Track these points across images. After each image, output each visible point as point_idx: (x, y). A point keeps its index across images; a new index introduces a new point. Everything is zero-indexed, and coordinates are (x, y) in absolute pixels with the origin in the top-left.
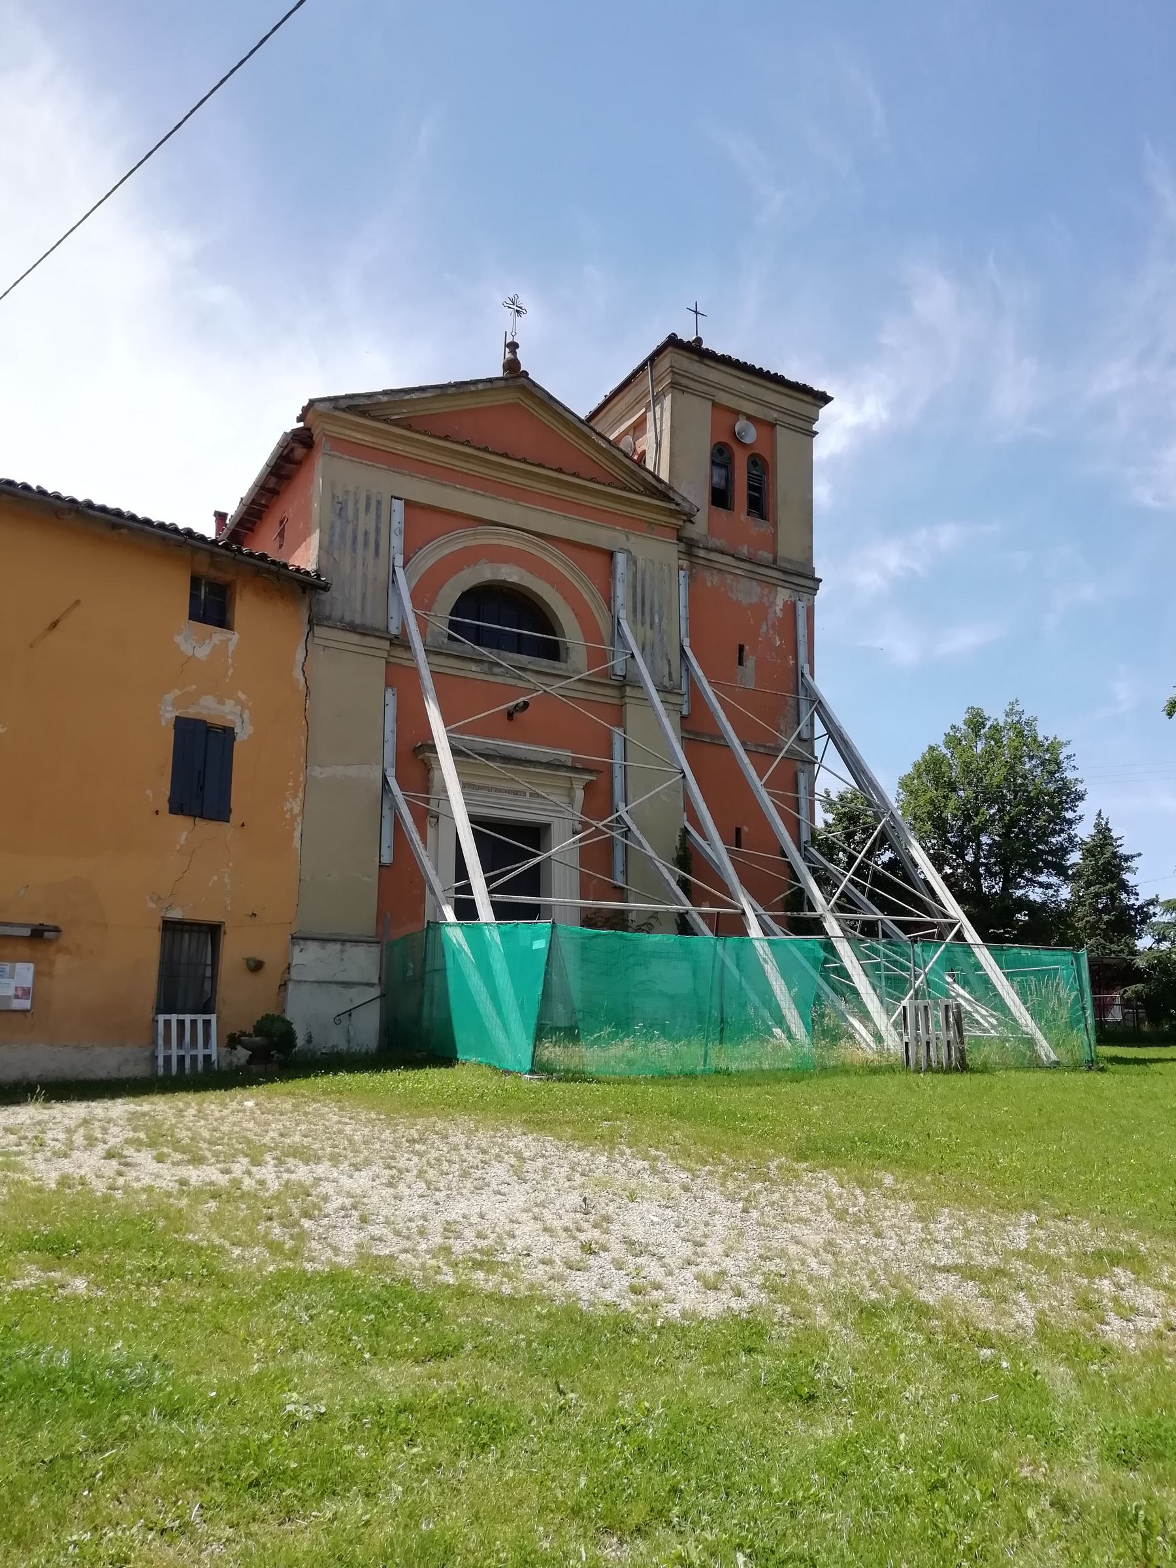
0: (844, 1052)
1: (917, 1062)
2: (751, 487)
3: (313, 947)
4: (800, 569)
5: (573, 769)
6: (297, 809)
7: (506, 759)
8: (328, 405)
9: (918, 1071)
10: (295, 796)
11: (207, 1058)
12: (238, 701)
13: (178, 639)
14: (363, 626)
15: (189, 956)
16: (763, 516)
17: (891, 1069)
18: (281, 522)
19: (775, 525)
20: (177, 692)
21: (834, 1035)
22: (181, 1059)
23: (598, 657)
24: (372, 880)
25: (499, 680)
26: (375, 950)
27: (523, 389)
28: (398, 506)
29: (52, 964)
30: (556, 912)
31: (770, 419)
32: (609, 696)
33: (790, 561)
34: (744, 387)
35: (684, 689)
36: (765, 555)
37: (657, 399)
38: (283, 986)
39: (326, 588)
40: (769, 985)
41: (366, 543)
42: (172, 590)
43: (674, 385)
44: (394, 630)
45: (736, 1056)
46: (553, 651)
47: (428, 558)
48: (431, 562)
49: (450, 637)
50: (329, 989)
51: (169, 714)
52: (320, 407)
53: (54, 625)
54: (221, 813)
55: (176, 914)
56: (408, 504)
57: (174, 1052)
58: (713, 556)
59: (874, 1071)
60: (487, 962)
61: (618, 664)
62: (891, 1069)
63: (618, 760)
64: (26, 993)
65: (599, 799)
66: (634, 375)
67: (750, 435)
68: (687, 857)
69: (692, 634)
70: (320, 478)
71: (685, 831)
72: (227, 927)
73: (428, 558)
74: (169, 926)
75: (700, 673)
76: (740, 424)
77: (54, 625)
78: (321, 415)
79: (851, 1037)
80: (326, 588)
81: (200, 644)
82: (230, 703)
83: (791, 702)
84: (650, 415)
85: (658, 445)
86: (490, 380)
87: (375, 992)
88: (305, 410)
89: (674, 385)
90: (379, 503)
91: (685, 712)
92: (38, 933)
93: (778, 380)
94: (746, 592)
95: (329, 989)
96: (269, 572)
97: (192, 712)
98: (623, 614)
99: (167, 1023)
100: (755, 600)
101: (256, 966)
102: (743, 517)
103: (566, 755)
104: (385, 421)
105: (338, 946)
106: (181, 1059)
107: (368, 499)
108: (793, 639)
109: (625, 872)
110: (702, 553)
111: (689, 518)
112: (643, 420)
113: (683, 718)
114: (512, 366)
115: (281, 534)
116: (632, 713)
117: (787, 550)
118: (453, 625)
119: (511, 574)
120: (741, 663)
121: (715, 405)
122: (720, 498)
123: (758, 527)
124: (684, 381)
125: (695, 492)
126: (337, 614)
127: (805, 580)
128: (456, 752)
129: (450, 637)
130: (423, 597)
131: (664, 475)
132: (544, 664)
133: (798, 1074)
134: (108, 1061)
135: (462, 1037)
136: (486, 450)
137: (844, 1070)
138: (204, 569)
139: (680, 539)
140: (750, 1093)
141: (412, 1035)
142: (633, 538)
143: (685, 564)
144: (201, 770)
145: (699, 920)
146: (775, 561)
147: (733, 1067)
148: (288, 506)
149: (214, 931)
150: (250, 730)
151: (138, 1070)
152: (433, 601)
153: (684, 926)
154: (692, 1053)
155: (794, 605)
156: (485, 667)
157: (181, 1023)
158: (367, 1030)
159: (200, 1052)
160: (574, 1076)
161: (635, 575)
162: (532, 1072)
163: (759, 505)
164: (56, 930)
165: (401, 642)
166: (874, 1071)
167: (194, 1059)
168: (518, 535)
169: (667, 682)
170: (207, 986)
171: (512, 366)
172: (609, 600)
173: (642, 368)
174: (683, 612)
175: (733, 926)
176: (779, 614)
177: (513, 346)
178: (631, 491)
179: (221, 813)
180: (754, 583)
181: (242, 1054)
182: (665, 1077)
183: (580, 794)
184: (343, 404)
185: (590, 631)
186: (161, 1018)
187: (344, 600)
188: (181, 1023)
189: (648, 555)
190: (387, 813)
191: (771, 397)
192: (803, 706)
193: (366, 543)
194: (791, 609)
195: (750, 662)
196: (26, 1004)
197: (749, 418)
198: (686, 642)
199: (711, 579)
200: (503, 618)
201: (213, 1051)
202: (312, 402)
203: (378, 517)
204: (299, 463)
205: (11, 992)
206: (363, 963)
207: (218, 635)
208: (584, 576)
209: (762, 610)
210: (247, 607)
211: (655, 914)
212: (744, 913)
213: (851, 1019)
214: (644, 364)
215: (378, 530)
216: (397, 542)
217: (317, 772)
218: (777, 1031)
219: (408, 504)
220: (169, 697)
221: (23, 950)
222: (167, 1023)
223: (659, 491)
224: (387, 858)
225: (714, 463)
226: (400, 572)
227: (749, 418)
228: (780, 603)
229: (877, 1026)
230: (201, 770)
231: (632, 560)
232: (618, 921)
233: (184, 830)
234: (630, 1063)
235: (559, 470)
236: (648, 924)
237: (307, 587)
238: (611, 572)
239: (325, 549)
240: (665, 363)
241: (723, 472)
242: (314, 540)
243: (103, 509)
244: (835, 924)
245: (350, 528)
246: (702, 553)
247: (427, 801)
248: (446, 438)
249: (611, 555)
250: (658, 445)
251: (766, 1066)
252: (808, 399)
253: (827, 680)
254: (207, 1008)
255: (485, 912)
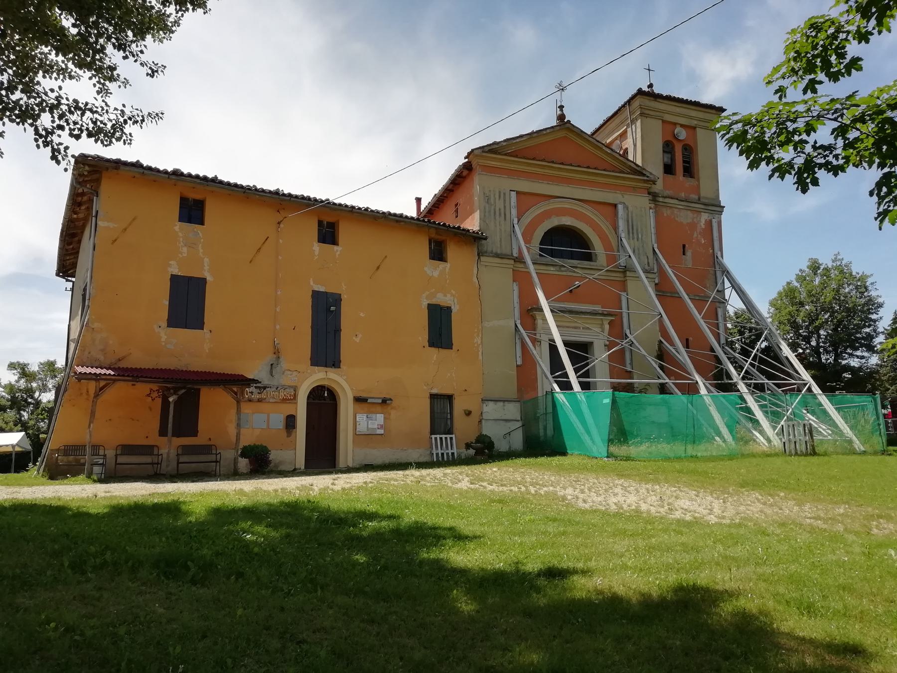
0: (752, 448)
1: (790, 451)
2: (684, 162)
3: (491, 404)
4: (713, 202)
5: (603, 314)
6: (479, 342)
7: (571, 312)
8: (480, 151)
9: (791, 455)
10: (478, 336)
11: (453, 454)
12: (452, 295)
13: (426, 269)
14: (501, 254)
15: (441, 408)
16: (692, 176)
17: (776, 455)
18: (456, 205)
19: (698, 181)
20: (427, 293)
21: (747, 440)
22: (442, 454)
23: (612, 259)
24: (514, 373)
25: (564, 273)
26: (518, 405)
27: (568, 128)
28: (513, 194)
29: (390, 414)
30: (598, 385)
31: (693, 125)
32: (618, 277)
33: (706, 198)
34: (678, 110)
35: (656, 270)
36: (694, 197)
37: (633, 122)
38: (480, 422)
39: (486, 239)
40: (712, 417)
41: (500, 214)
42: (422, 247)
43: (642, 114)
44: (515, 255)
45: (701, 450)
46: (589, 257)
47: (528, 218)
48: (529, 219)
49: (541, 255)
50: (501, 421)
51: (425, 303)
52: (476, 152)
53: (378, 268)
54: (449, 346)
55: (435, 391)
56: (518, 193)
57: (440, 452)
58: (667, 200)
59: (768, 455)
60: (583, 410)
61: (622, 261)
62: (776, 455)
63: (624, 310)
64: (382, 426)
65: (617, 330)
66: (620, 109)
67: (682, 134)
68: (662, 355)
69: (658, 242)
70: (478, 185)
71: (661, 342)
72: (455, 396)
73: (528, 218)
74: (433, 397)
75: (664, 262)
76: (678, 130)
77: (378, 268)
78: (477, 156)
79: (755, 441)
80: (486, 239)
81: (435, 269)
82: (449, 295)
83: (712, 272)
84: (629, 130)
85: (635, 145)
86: (552, 127)
87: (519, 424)
88: (469, 154)
89: (642, 114)
90: (504, 194)
91: (657, 281)
92: (384, 401)
93: (697, 104)
94: (684, 217)
95: (501, 421)
96: (462, 234)
97: (434, 301)
98: (623, 235)
99: (436, 439)
100: (689, 221)
101: (468, 413)
102: (681, 178)
103: (598, 308)
104: (505, 155)
105: (501, 404)
106: (442, 454)
107: (500, 192)
108: (711, 237)
109: (631, 364)
110: (661, 199)
111: (654, 182)
112: (625, 132)
113: (656, 284)
114: (561, 117)
115: (457, 211)
116: (630, 284)
117: (705, 192)
118: (541, 249)
119: (567, 221)
120: (684, 254)
121: (664, 122)
122: (669, 169)
123: (689, 182)
124: (647, 112)
125: (656, 169)
126: (490, 249)
127: (716, 207)
128: (552, 311)
129: (541, 255)
130: (527, 238)
131: (639, 162)
132: (586, 264)
133: (731, 457)
134: (415, 455)
135: (569, 443)
136: (553, 162)
137: (753, 456)
138: (433, 236)
139: (649, 193)
140: (711, 465)
141: (542, 441)
142: (626, 196)
143: (652, 206)
144: (440, 327)
145: (673, 386)
146: (699, 199)
147: (699, 455)
148: (460, 197)
149: (450, 398)
150: (457, 307)
151: (422, 460)
152: (531, 239)
153: (663, 389)
154: (678, 448)
155: (711, 221)
156: (558, 268)
157: (441, 439)
158: (517, 441)
159: (450, 452)
160: (628, 459)
161: (628, 215)
162: (608, 457)
163: (689, 170)
164: (391, 400)
165: (520, 260)
166: (768, 455)
167: (448, 454)
168: (570, 201)
169: (647, 267)
170: (449, 422)
171: (561, 117)
172: (616, 228)
173: (624, 106)
174: (653, 231)
175: (691, 389)
176: (703, 226)
177: (561, 107)
178: (624, 173)
179: (449, 346)
180: (689, 212)
181: (472, 452)
182: (667, 459)
183: (607, 327)
184: (487, 149)
185: (607, 246)
186: (433, 436)
187: (493, 243)
188: (441, 439)
189: (635, 204)
190: (518, 342)
191: (694, 113)
192: (719, 274)
193: (500, 214)
194: (709, 224)
195: (689, 253)
196: (382, 432)
197: (682, 126)
198: (656, 246)
199: (666, 212)
200: (564, 243)
201: (455, 450)
202: (473, 150)
203: (505, 201)
204: (465, 177)
205: (376, 427)
206: (513, 411)
207: (442, 265)
208: (601, 217)
209: (693, 226)
210: (453, 251)
211: (648, 384)
212: (697, 382)
213: (754, 432)
214: (625, 104)
215: (505, 207)
216: (514, 212)
217: (486, 324)
218: (717, 438)
219: (518, 193)
220: (424, 295)
221: (379, 408)
222: (436, 439)
223: (638, 171)
224: (519, 362)
225: (664, 152)
226: (516, 226)
227: (682, 126)
228: (703, 221)
229: (768, 434)
230: (440, 327)
231: (626, 208)
232: (629, 388)
233: (435, 354)
234: (650, 453)
235: (588, 167)
236: (644, 390)
237: (474, 239)
238: (616, 214)
239: (483, 219)
240: (636, 103)
241: (669, 156)
242: (477, 215)
243: (395, 215)
244: (743, 386)
245: (493, 208)
246: (661, 199)
247: (535, 334)
248: (534, 159)
249: (615, 206)
250: (635, 145)
251: (714, 454)
252: (714, 111)
253: (730, 259)
254: (450, 432)
255: (576, 387)
